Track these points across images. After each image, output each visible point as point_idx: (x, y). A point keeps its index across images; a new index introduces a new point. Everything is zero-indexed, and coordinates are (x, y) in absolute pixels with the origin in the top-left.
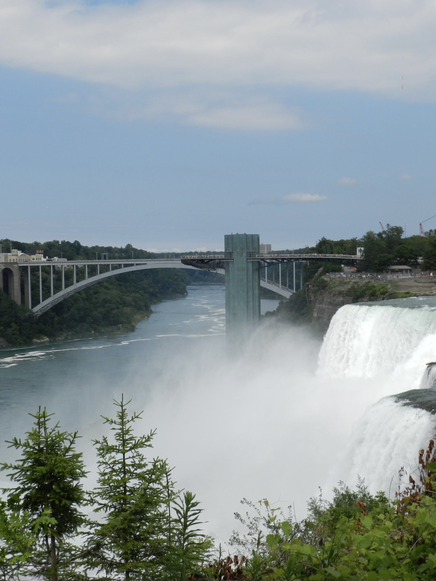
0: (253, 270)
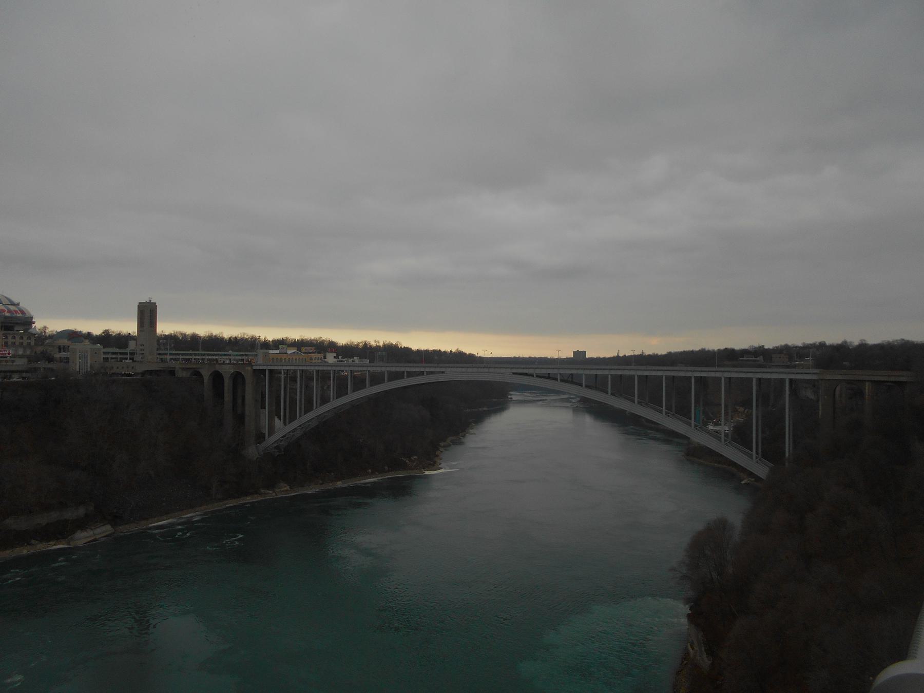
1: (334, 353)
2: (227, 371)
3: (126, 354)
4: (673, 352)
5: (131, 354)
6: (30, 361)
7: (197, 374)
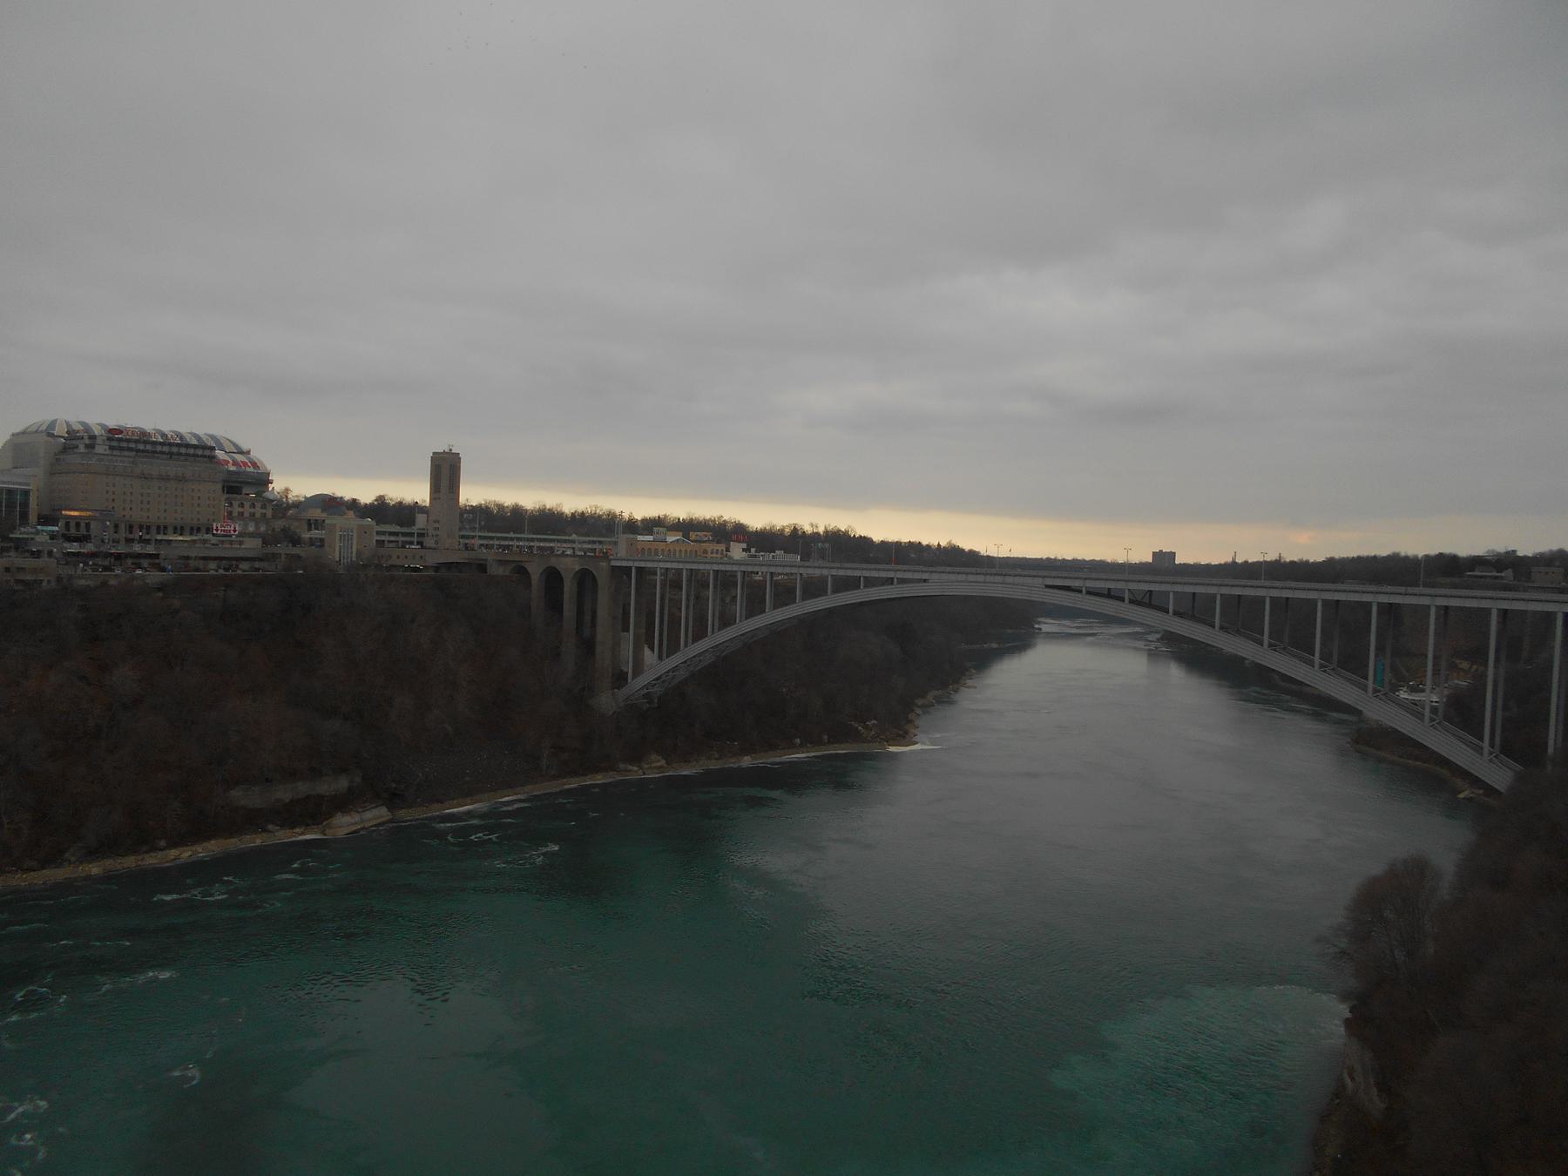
1: (743, 542)
2: (569, 566)
3: (412, 535)
4: (1337, 557)
5: (421, 535)
6: (265, 543)
7: (521, 571)
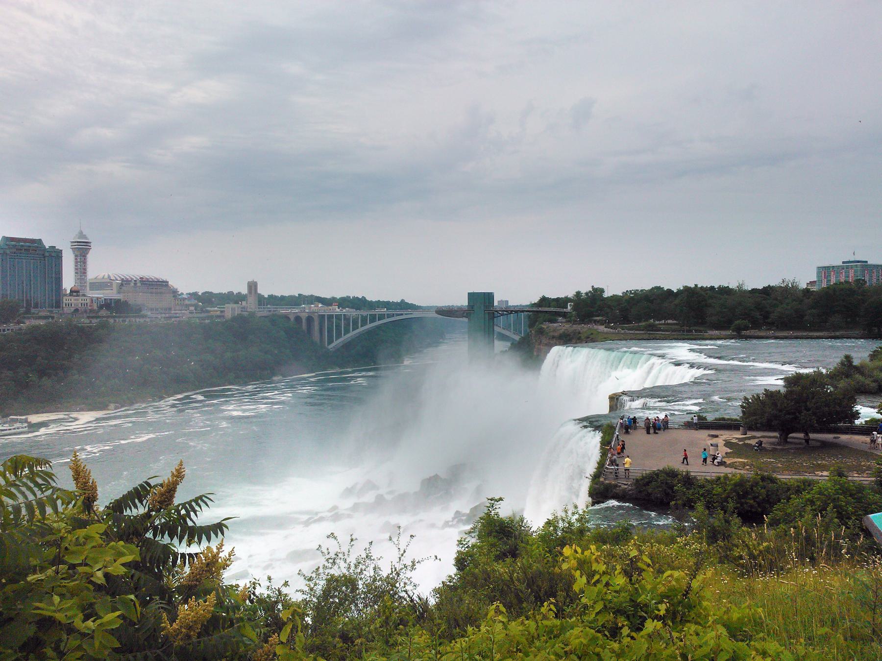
0: (489, 320)
2: (304, 316)
